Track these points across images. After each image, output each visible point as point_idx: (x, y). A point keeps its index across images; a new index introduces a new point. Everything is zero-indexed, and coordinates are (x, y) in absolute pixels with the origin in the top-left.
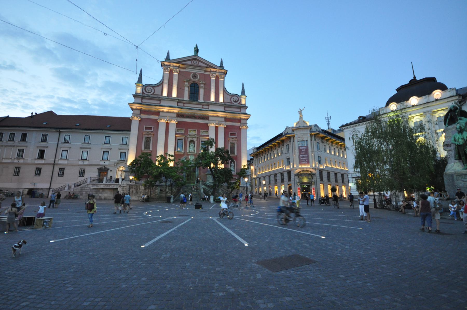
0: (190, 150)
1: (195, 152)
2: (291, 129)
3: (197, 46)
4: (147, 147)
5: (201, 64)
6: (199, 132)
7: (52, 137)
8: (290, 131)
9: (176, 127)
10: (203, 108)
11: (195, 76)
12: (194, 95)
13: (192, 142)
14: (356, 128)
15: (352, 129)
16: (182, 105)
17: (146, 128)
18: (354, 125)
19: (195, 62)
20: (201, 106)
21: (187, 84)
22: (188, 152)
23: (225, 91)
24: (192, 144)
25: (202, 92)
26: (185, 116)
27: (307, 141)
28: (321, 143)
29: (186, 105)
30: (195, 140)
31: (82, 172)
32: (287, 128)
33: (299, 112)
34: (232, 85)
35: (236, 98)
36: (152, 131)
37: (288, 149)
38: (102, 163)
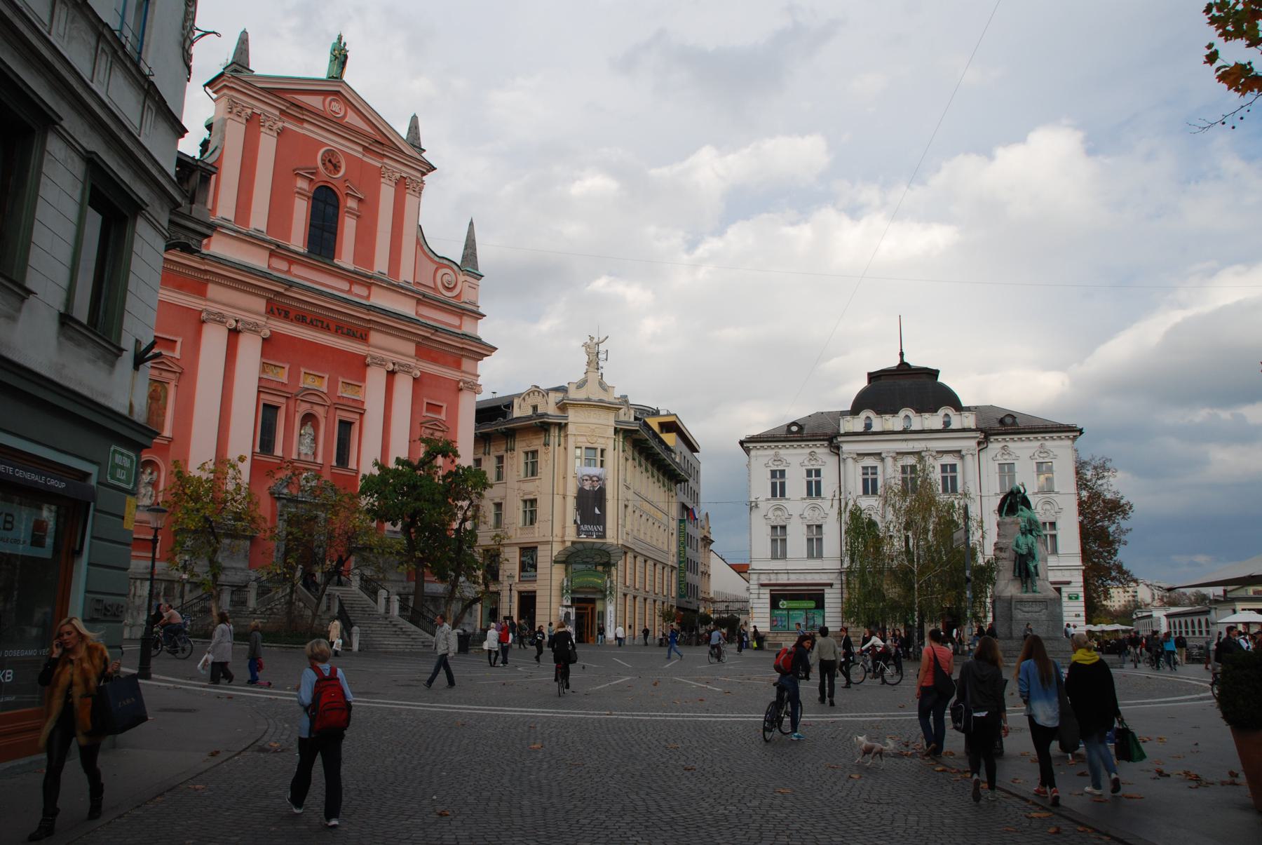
0: (304, 450)
1: (319, 460)
2: (554, 398)
3: (340, 38)
5: (352, 119)
6: (333, 384)
8: (549, 408)
9: (263, 354)
10: (349, 291)
11: (331, 161)
13: (309, 418)
14: (782, 452)
15: (773, 452)
16: (283, 265)
18: (780, 444)
19: (336, 107)
20: (345, 286)
21: (302, 184)
22: (295, 456)
23: (421, 241)
24: (308, 429)
25: (349, 228)
26: (292, 315)
27: (602, 451)
28: (630, 460)
29: (296, 270)
30: (320, 412)
32: (535, 390)
33: (585, 345)
34: (439, 218)
35: (448, 275)
36: (177, 354)
37: (532, 469)
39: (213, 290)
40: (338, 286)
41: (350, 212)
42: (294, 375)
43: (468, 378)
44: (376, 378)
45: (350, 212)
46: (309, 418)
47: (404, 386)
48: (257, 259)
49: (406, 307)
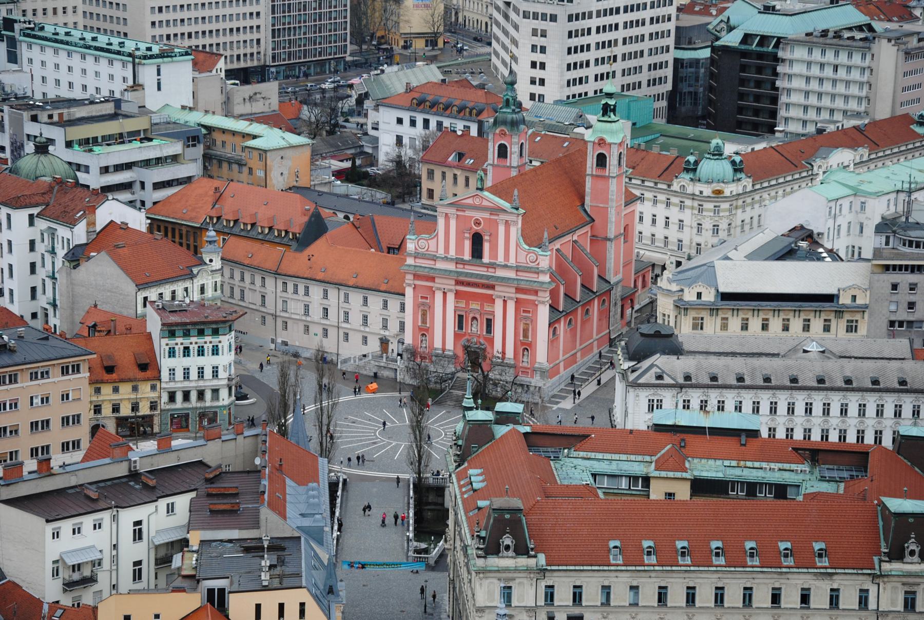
4: (424, 321)
6: (482, 306)
7: (333, 293)
9: (456, 298)
11: (478, 223)
12: (477, 252)
16: (462, 266)
17: (422, 297)
20: (485, 269)
21: (467, 235)
24: (475, 321)
25: (486, 246)
29: (466, 267)
30: (478, 316)
31: (365, 340)
38: (382, 332)
39: (437, 280)
40: (482, 271)
41: (487, 241)
42: (467, 304)
43: (540, 299)
44: (499, 304)
45: (487, 241)
46: (474, 318)
47: (511, 306)
48: (451, 267)
49: (511, 274)
